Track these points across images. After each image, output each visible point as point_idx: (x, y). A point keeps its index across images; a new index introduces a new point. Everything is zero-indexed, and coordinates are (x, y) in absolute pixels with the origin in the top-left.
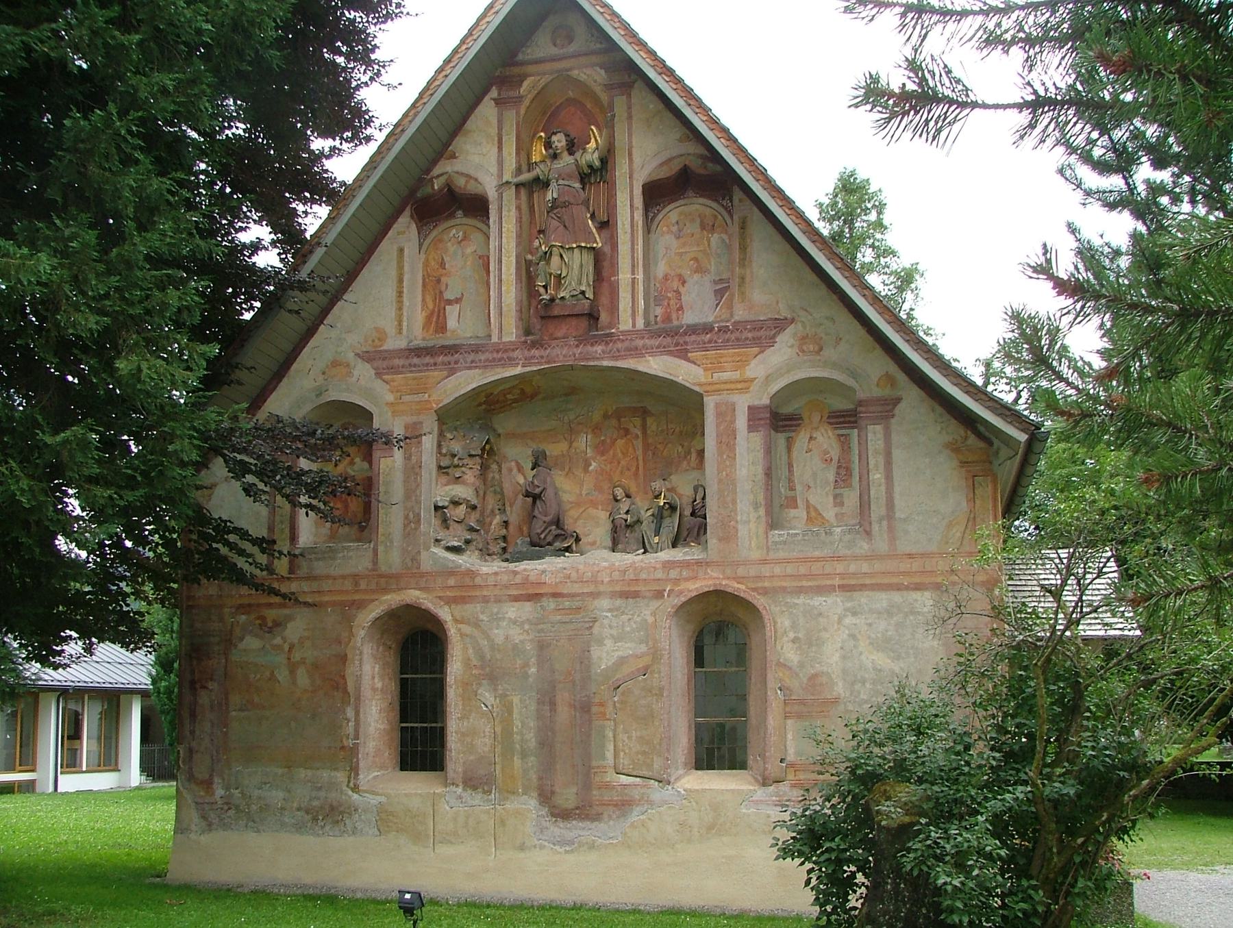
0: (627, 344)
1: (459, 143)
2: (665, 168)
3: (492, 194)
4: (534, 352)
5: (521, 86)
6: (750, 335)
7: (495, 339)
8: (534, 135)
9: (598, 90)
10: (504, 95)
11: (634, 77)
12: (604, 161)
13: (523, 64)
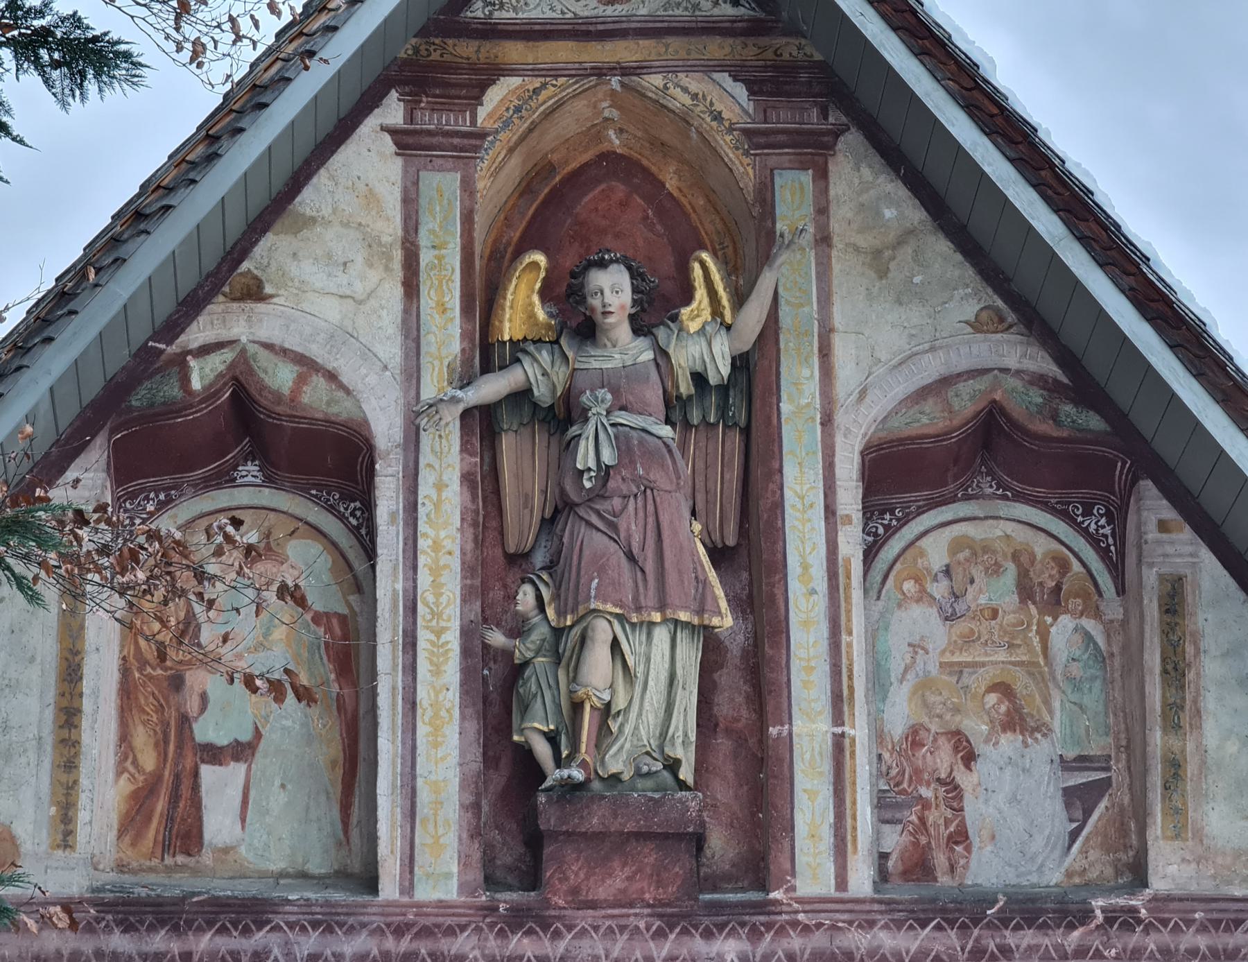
1: (272, 253)
2: (929, 405)
3: (386, 428)
5: (478, 99)
6: (1202, 942)
7: (389, 889)
9: (725, 143)
10: (428, 120)
11: (835, 117)
12: (741, 363)
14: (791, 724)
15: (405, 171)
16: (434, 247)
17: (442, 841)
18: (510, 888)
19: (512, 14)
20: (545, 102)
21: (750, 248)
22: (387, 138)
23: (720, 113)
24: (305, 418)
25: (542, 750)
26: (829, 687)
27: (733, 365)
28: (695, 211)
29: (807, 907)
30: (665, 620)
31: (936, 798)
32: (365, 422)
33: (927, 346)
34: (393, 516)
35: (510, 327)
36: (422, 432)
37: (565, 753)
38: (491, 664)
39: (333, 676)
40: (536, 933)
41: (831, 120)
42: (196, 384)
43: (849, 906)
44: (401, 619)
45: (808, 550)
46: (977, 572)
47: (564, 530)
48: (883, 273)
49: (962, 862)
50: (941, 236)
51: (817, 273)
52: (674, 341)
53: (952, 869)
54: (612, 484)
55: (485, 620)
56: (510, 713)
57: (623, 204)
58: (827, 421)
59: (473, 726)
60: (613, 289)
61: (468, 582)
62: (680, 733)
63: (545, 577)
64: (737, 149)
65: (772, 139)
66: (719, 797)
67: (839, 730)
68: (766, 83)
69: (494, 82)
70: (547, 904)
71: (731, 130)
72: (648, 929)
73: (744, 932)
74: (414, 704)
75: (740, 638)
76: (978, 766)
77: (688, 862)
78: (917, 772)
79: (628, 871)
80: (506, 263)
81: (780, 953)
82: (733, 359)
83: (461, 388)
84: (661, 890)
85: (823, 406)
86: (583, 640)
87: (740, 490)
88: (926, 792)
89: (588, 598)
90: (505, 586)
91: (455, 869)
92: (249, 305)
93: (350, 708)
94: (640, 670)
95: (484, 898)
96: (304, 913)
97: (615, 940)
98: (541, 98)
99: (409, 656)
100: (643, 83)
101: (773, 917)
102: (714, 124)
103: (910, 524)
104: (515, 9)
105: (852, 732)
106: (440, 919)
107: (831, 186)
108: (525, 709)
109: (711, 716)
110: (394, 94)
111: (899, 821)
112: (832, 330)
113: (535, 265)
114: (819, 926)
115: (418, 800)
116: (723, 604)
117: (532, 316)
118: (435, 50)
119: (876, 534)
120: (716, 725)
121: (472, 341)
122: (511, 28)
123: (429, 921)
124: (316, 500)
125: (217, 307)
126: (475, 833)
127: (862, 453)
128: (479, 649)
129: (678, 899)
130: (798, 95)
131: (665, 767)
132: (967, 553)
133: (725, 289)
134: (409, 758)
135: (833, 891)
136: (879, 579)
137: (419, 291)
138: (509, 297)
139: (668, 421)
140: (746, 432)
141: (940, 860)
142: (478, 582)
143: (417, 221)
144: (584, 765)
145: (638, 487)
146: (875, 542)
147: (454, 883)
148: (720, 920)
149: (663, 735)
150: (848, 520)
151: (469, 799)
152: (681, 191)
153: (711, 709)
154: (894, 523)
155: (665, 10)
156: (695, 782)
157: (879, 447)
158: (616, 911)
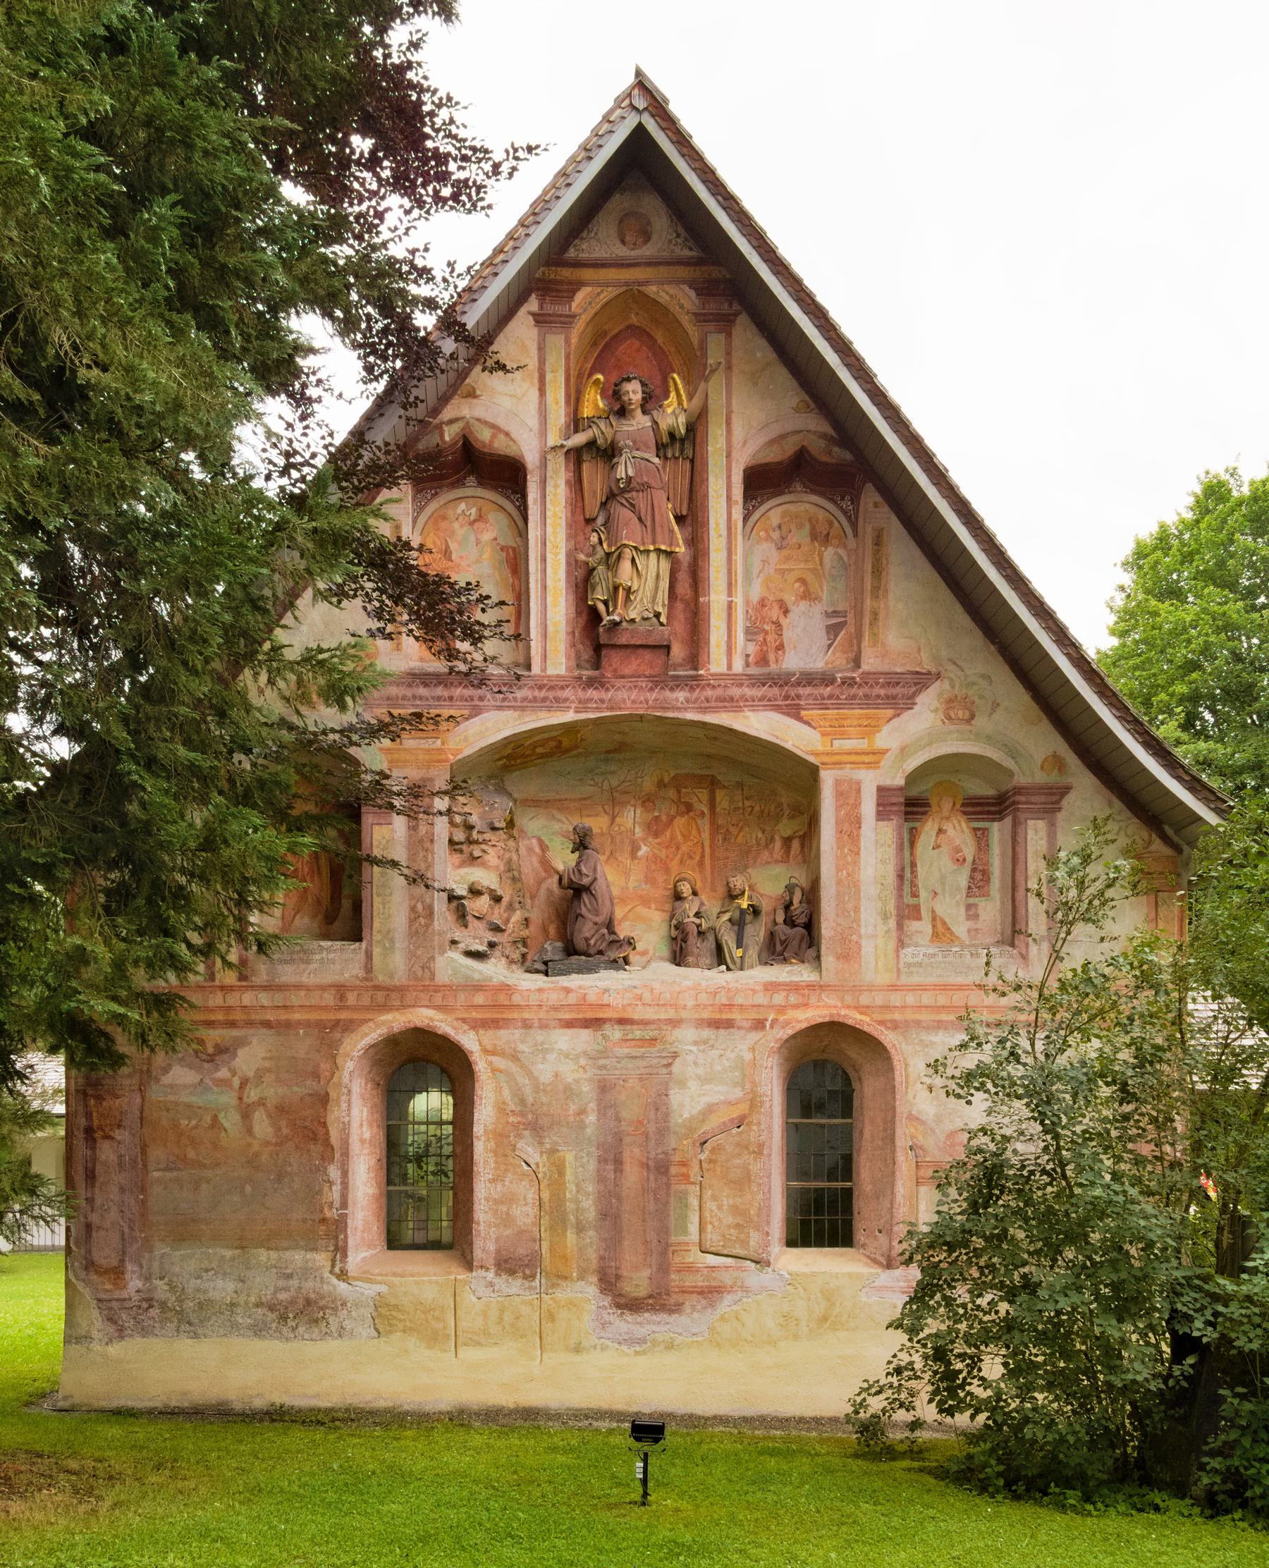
0: (719, 692)
3: (531, 458)
4: (591, 693)
5: (572, 298)
6: (882, 692)
7: (536, 669)
9: (685, 320)
10: (549, 309)
11: (736, 307)
12: (691, 428)
25: (601, 607)
35: (587, 412)
42: (447, 438)
46: (793, 527)
59: (572, 597)
60: (633, 391)
68: (705, 290)
70: (603, 676)
76: (790, 615)
86: (619, 557)
125: (455, 401)
140: (692, 461)
148: (679, 683)
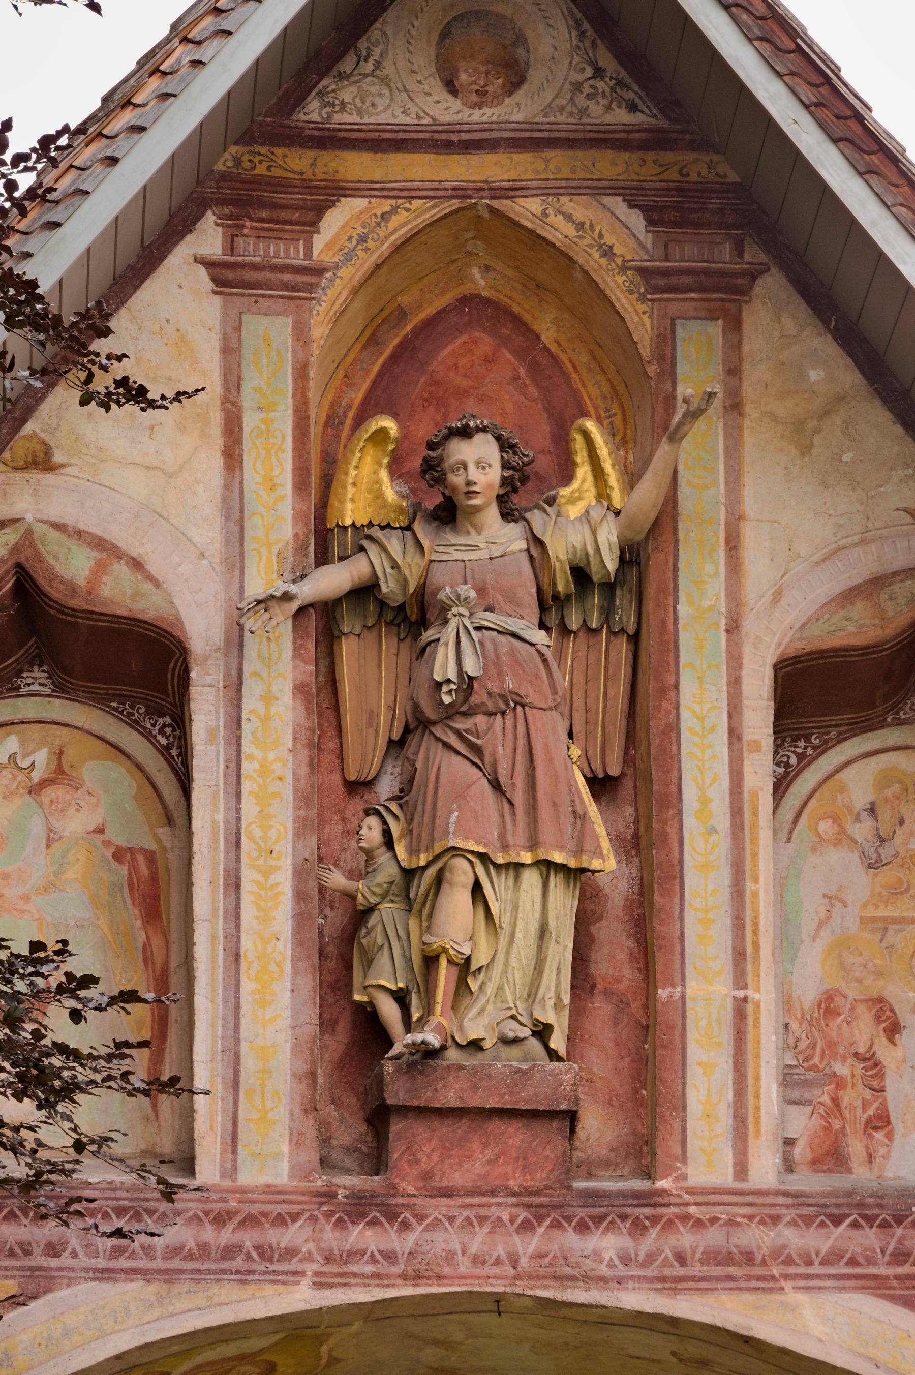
0: (714, 1237)
2: (859, 610)
3: (201, 627)
4: (360, 1236)
5: (313, 225)
7: (208, 1170)
8: (361, 420)
9: (617, 286)
10: (253, 250)
11: (753, 254)
12: (631, 556)
13: (330, 140)
14: (684, 985)
15: (225, 314)
16: (260, 409)
17: (270, 1115)
18: (348, 1171)
19: (355, 118)
20: (395, 231)
21: (648, 413)
22: (202, 272)
23: (611, 247)
24: (105, 615)
25: (389, 1010)
26: (729, 943)
27: (622, 560)
28: (576, 370)
29: (700, 1199)
30: (537, 863)
31: (853, 1076)
32: (179, 621)
33: (856, 539)
34: (212, 733)
35: (352, 509)
36: (247, 634)
37: (415, 1016)
38: (327, 911)
39: (138, 923)
40: (381, 1224)
41: (747, 257)
43: (749, 1199)
44: (222, 856)
45: (708, 781)
47: (416, 754)
48: (805, 450)
49: (882, 1151)
50: (878, 402)
51: (726, 448)
52: (550, 528)
53: (870, 1158)
54: (475, 699)
55: (320, 859)
56: (349, 968)
57: (489, 360)
58: (733, 628)
59: (308, 983)
60: (478, 463)
61: (302, 813)
62: (552, 994)
63: (394, 807)
64: (631, 292)
65: (674, 280)
66: (595, 1070)
67: (741, 994)
68: (668, 210)
69: (331, 204)
70: (393, 1190)
71: (624, 269)
72: (512, 1222)
73: (625, 1226)
74: (237, 956)
75: (623, 885)
76: (903, 1039)
77: (559, 1143)
78: (831, 1045)
79: (489, 1153)
80: (346, 431)
81: (668, 1252)
82: (622, 550)
83: (294, 582)
84: (528, 1177)
85: (729, 611)
86: (439, 881)
87: (626, 707)
88: (841, 1069)
89: (446, 833)
90: (344, 820)
91: (285, 1149)
92: (35, 476)
93: (159, 959)
94: (506, 921)
95: (319, 1183)
96: (107, 1199)
97: (473, 1234)
98: (392, 225)
99: (232, 900)
100: (517, 208)
101: (660, 1210)
102: (604, 261)
103: (828, 753)
104: (360, 113)
105: (757, 996)
106: (267, 1208)
107: (745, 341)
108: (368, 963)
109: (587, 975)
110: (210, 218)
111: (809, 1102)
112: (741, 518)
113: (383, 431)
114: (714, 1220)
115: (242, 1068)
116: (605, 844)
117: (379, 496)
118: (260, 162)
119: (787, 765)
120: (593, 987)
121: (307, 524)
122: (354, 135)
123: (255, 1209)
124: (117, 713)
126: (311, 1108)
127: (775, 666)
128: (315, 893)
129: (548, 1187)
130: (708, 225)
131: (534, 1034)
132: (896, 788)
133: (613, 466)
134: (231, 1019)
135: (730, 1178)
136: (790, 817)
137: (242, 462)
138: (353, 472)
139: (542, 626)
140: (635, 639)
141: (855, 1147)
142: (314, 813)
143: (239, 378)
144: (439, 1029)
145: (507, 704)
146: (786, 774)
147: (284, 1167)
149: (532, 995)
150: (756, 746)
151: (302, 1067)
152: (559, 345)
153: (587, 967)
154: (810, 751)
155: (545, 116)
156: (568, 1052)
157: (796, 659)
158: (476, 1200)
